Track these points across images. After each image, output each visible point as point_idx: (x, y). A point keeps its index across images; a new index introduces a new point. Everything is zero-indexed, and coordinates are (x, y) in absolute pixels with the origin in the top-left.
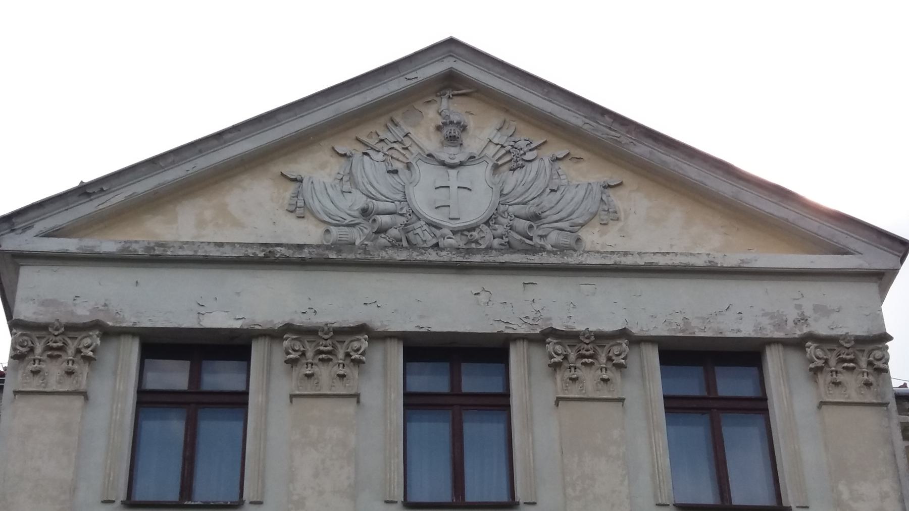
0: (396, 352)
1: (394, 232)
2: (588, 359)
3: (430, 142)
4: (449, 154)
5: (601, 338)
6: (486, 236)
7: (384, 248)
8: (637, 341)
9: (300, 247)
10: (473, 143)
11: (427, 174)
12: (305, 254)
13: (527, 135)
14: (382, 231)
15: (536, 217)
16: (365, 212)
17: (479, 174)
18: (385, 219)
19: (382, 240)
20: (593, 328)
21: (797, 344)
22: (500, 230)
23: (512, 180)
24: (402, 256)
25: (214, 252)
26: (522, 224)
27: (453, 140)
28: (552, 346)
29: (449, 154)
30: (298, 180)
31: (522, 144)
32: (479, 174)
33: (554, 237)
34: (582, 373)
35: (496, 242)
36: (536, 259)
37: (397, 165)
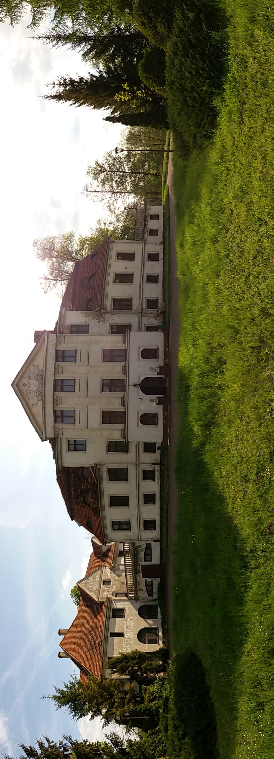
0: (55, 392)
1: (39, 393)
2: (57, 370)
3: (26, 388)
4: (28, 385)
5: (55, 368)
6: (40, 381)
7: (42, 394)
8: (55, 364)
9: (42, 404)
10: (27, 383)
11: (31, 388)
12: (43, 403)
13: (26, 375)
14: (39, 394)
15: (38, 375)
16: (37, 396)
17: (31, 381)
18: (38, 394)
19: (41, 394)
20: (53, 369)
21: (56, 345)
22: (39, 379)
23: (32, 377)
24: (43, 392)
25: (44, 415)
26: (39, 377)
27: (26, 385)
28: (56, 374)
29: (28, 385)
30: (32, 405)
31: (27, 376)
32: (31, 381)
33: (40, 373)
34: (59, 371)
35: (41, 380)
36: (44, 375)
37: (30, 392)
